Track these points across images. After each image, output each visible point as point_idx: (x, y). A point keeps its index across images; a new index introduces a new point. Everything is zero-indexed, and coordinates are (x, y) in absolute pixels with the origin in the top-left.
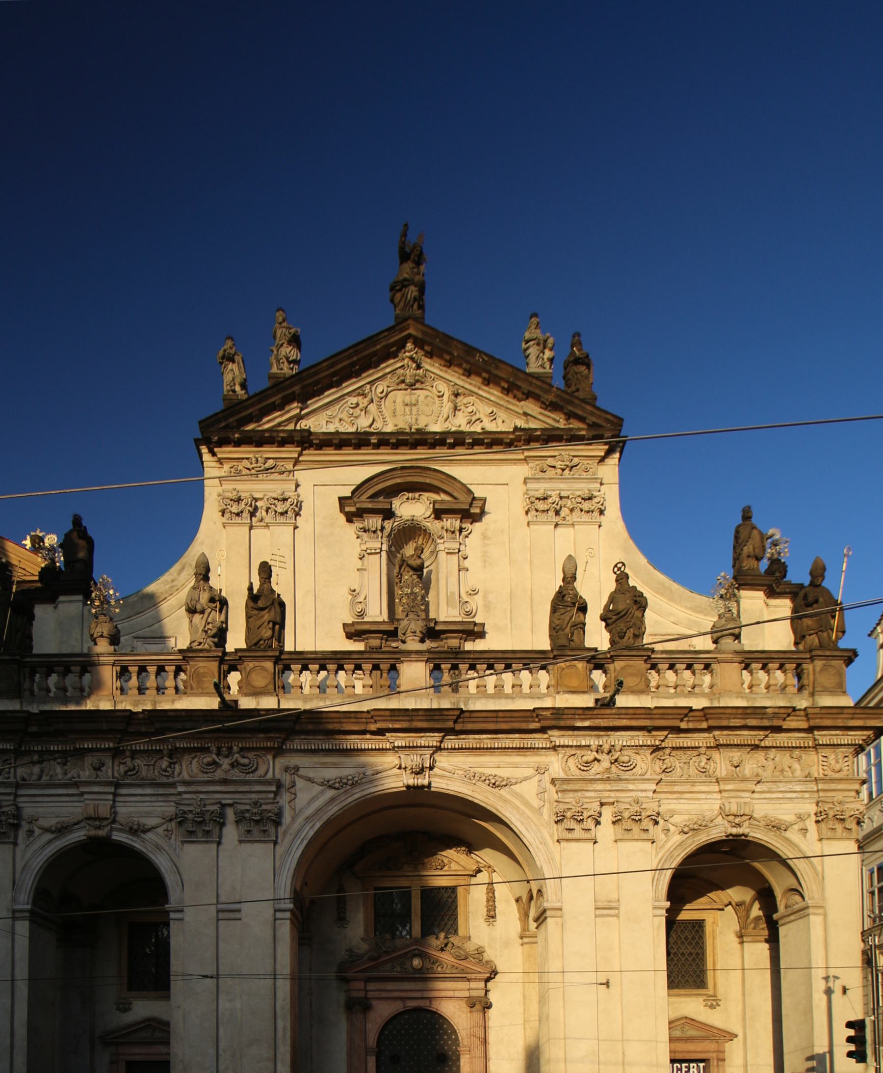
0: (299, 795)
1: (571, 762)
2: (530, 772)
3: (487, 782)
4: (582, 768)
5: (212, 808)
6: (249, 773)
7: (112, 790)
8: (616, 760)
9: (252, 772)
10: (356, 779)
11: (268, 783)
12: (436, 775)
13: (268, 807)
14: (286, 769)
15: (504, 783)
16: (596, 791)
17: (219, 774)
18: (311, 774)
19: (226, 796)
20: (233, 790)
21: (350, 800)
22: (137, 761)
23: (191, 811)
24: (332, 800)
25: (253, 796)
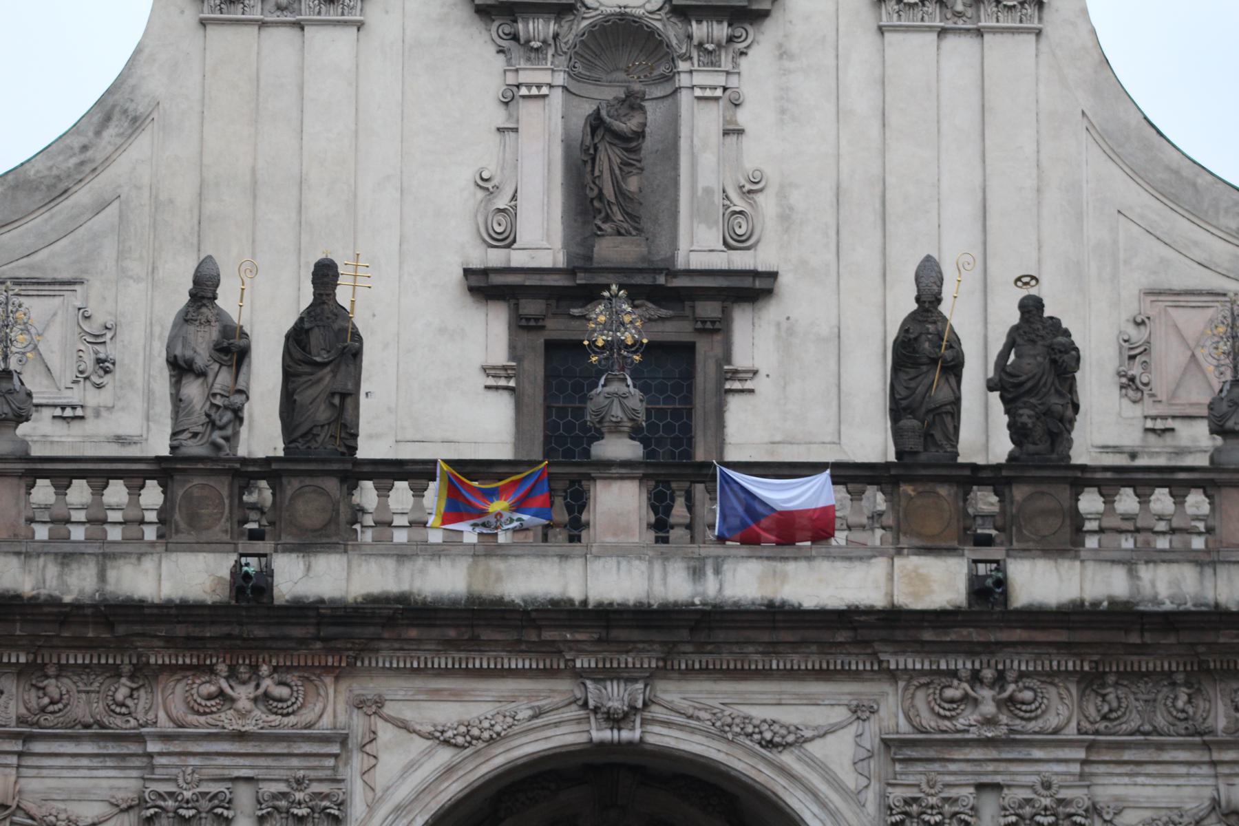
0: (384, 758)
1: (921, 695)
2: (840, 714)
3: (757, 737)
4: (942, 712)
5: (213, 788)
6: (288, 714)
7: (18, 746)
8: (1011, 700)
9: (293, 713)
10: (498, 728)
11: (325, 739)
12: (654, 721)
13: (324, 788)
14: (360, 704)
15: (791, 738)
16: (968, 761)
17: (228, 720)
18: (408, 713)
19: (241, 761)
20: (257, 750)
21: (484, 769)
22: (66, 680)
23: (171, 794)
24: (449, 770)
25: (295, 762)
